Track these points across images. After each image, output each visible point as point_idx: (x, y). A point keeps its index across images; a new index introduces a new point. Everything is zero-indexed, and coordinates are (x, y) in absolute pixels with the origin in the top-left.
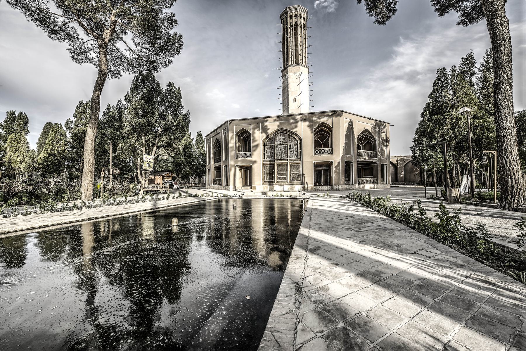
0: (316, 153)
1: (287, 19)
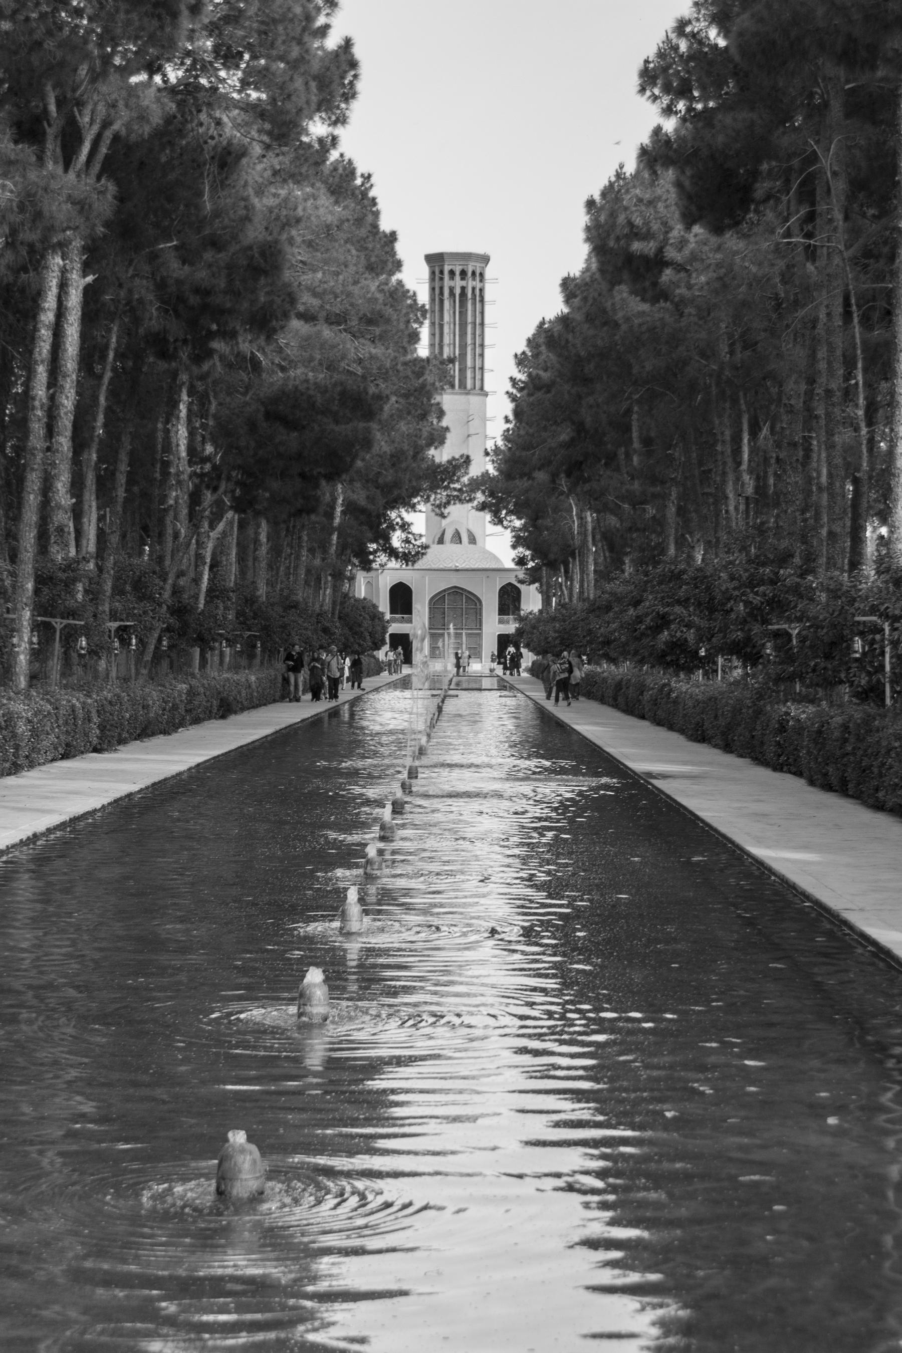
0: (501, 622)
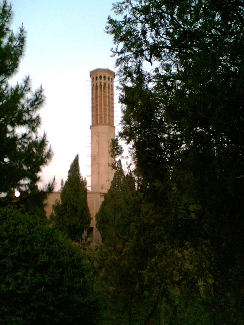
1: (97, 78)
